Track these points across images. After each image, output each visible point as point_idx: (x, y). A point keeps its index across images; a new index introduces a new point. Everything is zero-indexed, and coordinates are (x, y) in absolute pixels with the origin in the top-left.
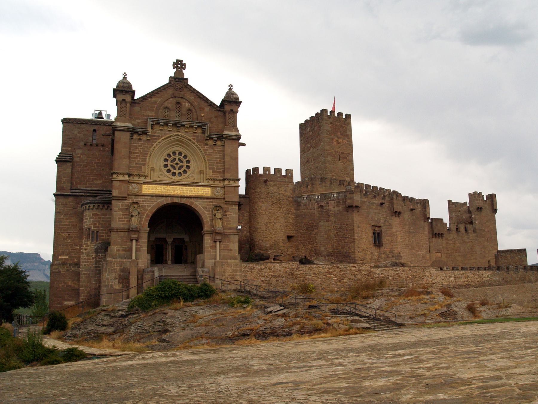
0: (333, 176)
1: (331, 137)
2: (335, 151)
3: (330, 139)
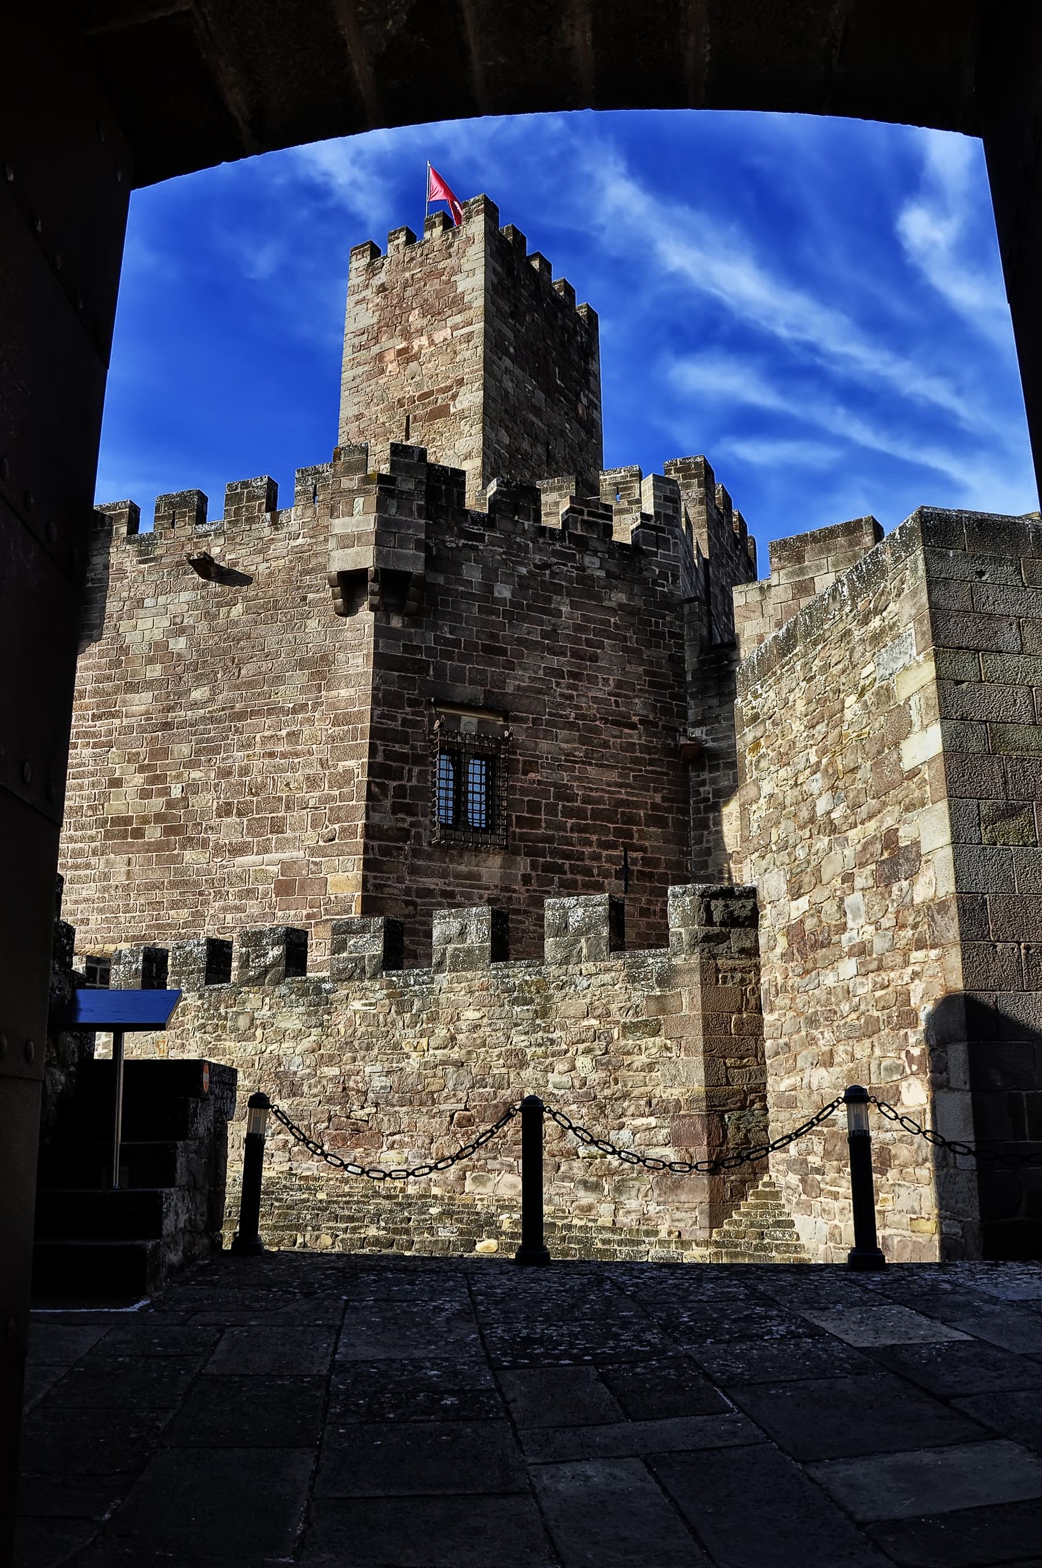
1: (375, 350)
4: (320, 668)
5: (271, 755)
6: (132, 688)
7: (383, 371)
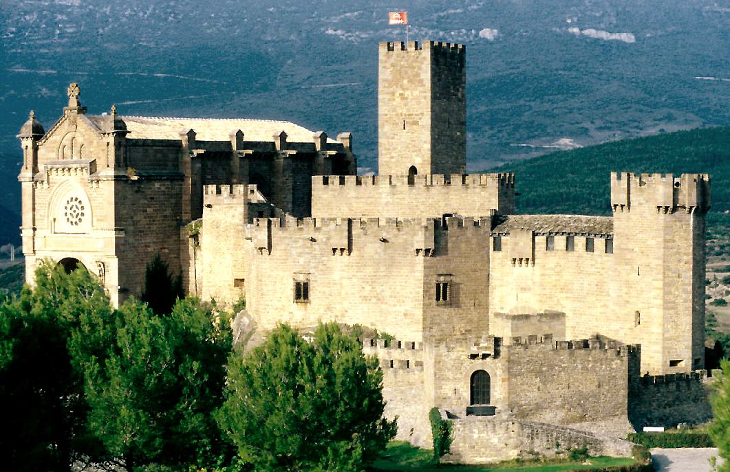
0: (392, 157)
1: (391, 90)
2: (397, 115)
3: (387, 93)
4: (412, 265)
6: (365, 266)
7: (394, 100)
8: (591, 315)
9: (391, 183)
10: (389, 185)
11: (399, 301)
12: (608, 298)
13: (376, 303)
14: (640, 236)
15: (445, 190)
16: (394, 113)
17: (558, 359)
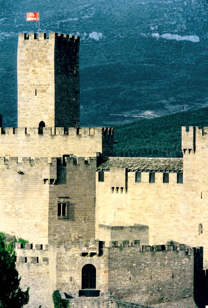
0: (27, 115)
1: (26, 67)
2: (31, 85)
3: (23, 70)
5: (33, 205)
6: (8, 191)
8: (167, 227)
9: (26, 133)
10: (24, 135)
11: (31, 216)
12: (180, 215)
13: (15, 217)
14: (202, 170)
15: (64, 138)
16: (29, 84)
17: (144, 258)
